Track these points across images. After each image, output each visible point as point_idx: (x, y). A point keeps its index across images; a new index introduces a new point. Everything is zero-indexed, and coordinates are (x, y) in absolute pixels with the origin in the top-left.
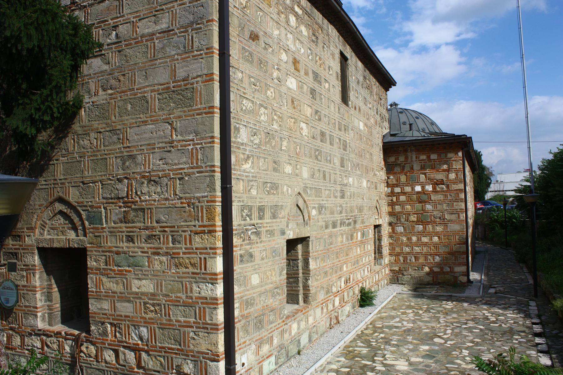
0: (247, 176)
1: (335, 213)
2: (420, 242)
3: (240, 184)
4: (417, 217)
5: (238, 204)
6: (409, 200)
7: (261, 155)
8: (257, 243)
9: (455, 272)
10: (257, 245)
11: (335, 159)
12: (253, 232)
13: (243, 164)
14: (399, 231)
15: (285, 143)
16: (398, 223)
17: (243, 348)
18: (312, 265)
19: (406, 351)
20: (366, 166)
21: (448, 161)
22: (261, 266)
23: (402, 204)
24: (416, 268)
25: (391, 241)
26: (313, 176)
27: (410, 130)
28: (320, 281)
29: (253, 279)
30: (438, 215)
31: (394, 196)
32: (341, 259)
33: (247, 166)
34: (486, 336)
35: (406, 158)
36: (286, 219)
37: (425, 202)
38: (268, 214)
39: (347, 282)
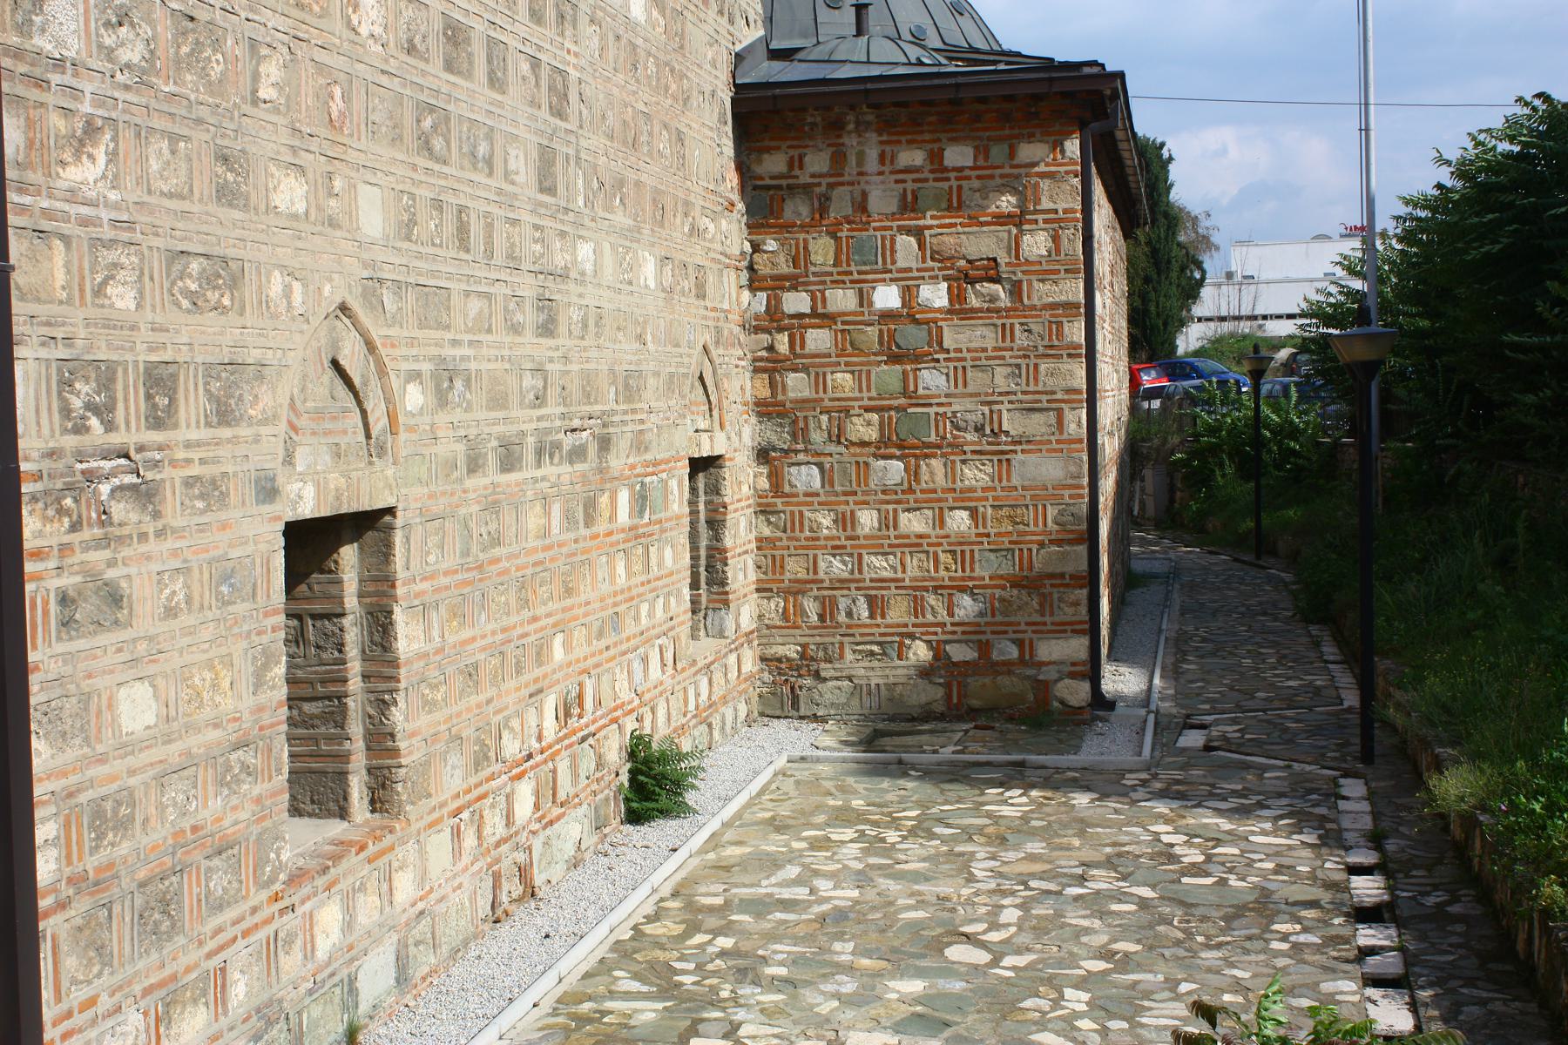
0: (85, 222)
1: (514, 399)
2: (892, 533)
3: (50, 259)
4: (881, 424)
5: (43, 353)
6: (849, 348)
7: (157, 123)
8: (143, 537)
9: (1042, 664)
10: (143, 548)
11: (513, 152)
12: (121, 488)
13: (63, 163)
14: (801, 488)
15: (272, 70)
16: (796, 452)
17: (80, 1031)
18: (408, 638)
19: (828, 1006)
20: (657, 191)
21: (1017, 177)
22: (164, 646)
23: (815, 367)
24: (876, 648)
25: (767, 532)
26: (407, 228)
27: (860, 32)
28: (446, 712)
29: (124, 708)
31: (780, 330)
32: (541, 611)
33: (86, 173)
34: (1161, 928)
35: (839, 159)
36: (283, 427)
37: (917, 358)
38: (192, 404)
39: (568, 715)
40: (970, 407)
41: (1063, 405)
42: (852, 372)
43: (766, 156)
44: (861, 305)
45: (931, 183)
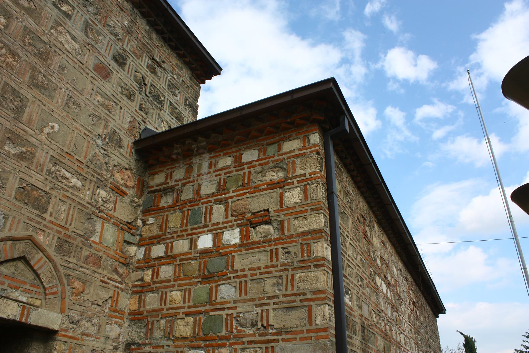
4: (195, 323)
16: (145, 344)
30: (249, 316)
31: (148, 268)
40: (248, 309)
41: (312, 303)
42: (181, 290)
43: (156, 176)
44: (191, 248)
45: (234, 173)
